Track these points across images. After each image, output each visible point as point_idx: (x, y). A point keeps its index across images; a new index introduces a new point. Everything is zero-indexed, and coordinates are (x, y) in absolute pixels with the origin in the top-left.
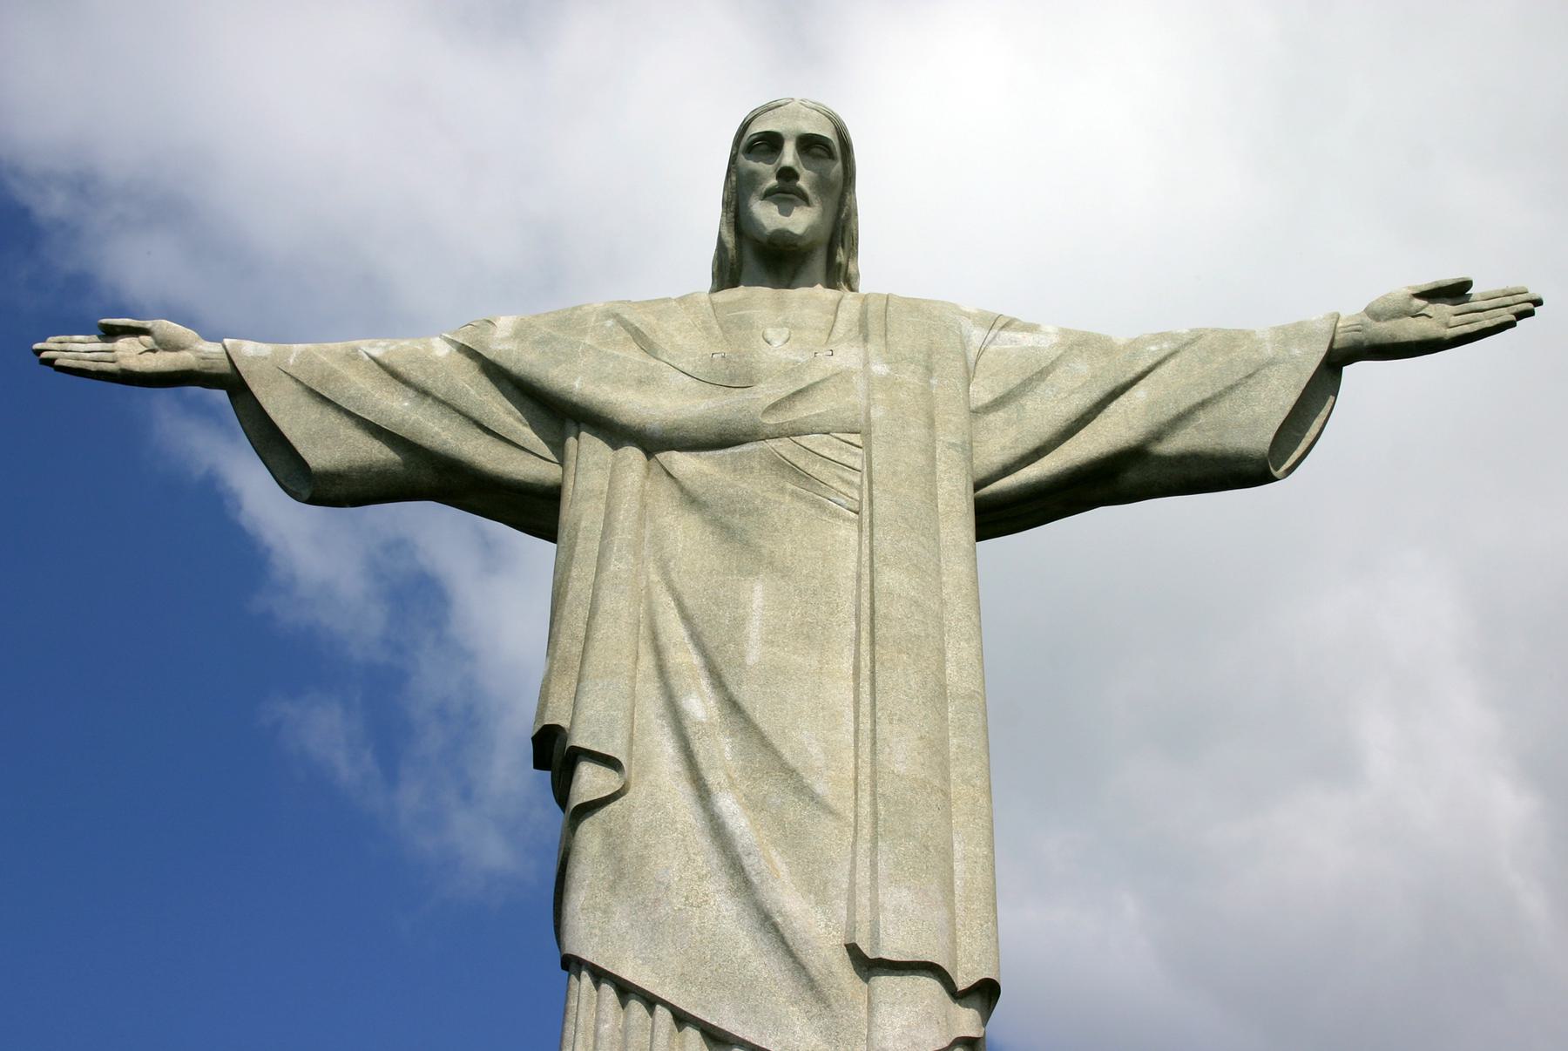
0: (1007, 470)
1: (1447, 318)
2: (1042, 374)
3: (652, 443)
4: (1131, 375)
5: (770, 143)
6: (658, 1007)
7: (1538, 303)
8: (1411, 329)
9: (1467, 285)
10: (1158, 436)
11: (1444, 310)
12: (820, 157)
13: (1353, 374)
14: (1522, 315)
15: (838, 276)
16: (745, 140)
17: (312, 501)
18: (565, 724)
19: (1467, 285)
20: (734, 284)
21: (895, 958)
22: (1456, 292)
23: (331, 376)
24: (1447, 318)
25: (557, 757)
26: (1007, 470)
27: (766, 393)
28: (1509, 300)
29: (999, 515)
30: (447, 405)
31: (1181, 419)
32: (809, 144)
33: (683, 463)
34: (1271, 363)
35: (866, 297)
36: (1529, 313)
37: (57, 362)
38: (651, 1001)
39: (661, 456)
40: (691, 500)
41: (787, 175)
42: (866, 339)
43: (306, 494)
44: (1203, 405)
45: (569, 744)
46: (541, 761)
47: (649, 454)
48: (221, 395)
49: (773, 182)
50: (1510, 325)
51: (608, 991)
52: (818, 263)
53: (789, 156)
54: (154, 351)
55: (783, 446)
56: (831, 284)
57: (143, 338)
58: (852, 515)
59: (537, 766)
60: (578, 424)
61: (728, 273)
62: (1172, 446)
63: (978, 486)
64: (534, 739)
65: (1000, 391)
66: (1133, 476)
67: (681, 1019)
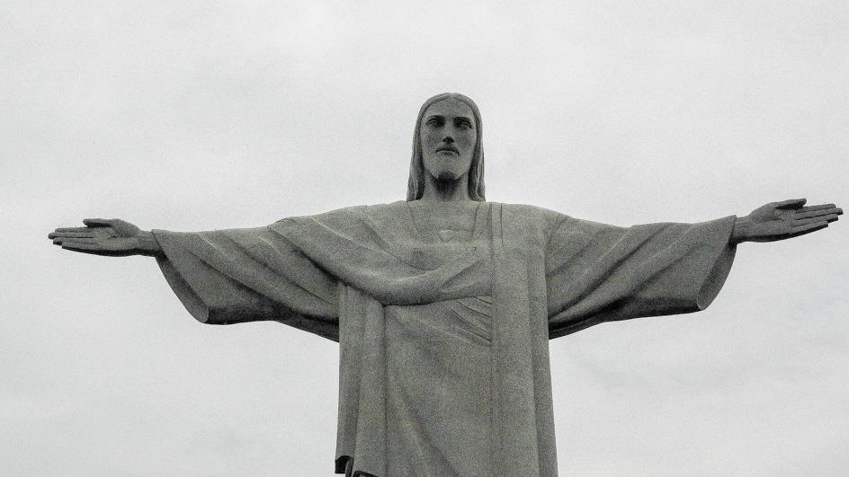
0: (564, 309)
1: (791, 220)
2: (581, 254)
3: (387, 301)
4: (627, 252)
5: (438, 122)
7: (842, 213)
8: (774, 227)
9: (804, 202)
10: (642, 287)
11: (792, 214)
12: (465, 128)
13: (743, 249)
14: (830, 221)
15: (475, 190)
16: (425, 120)
17: (209, 322)
18: (351, 456)
19: (804, 202)
20: (419, 197)
22: (797, 206)
23: (211, 251)
24: (791, 220)
27: (444, 274)
28: (824, 212)
29: (559, 328)
30: (275, 272)
31: (653, 279)
32: (461, 123)
33: (403, 314)
34: (702, 245)
35: (491, 205)
36: (837, 219)
37: (65, 244)
39: (392, 307)
40: (408, 335)
41: (449, 140)
42: (491, 238)
44: (663, 271)
45: (355, 469)
47: (384, 306)
48: (152, 260)
49: (442, 144)
50: (826, 226)
52: (464, 184)
53: (448, 130)
55: (451, 306)
56: (472, 195)
57: (111, 230)
58: (488, 343)
59: (336, 472)
61: (417, 192)
62: (649, 294)
63: (549, 318)
64: (336, 461)
65: (559, 263)
66: (627, 309)
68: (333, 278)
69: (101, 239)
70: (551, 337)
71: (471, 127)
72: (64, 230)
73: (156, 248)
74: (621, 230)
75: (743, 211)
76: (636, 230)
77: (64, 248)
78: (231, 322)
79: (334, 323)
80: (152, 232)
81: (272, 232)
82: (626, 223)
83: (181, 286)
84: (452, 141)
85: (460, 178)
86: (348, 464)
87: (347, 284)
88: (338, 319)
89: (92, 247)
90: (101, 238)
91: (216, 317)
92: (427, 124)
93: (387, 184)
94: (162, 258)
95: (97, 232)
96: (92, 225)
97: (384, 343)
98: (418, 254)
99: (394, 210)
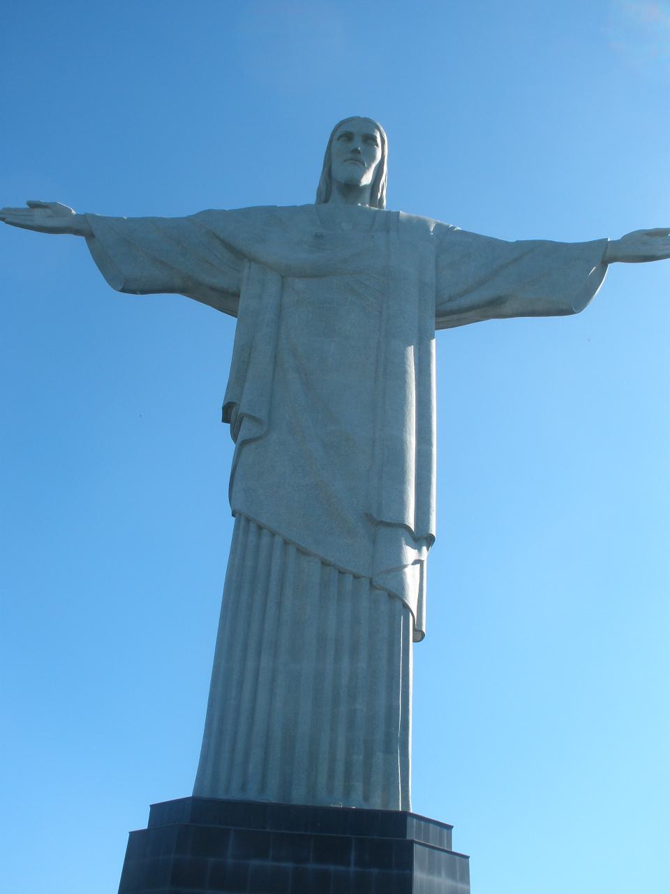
0: (451, 299)
3: (285, 274)
5: (349, 137)
6: (277, 536)
16: (338, 134)
20: (326, 201)
21: (389, 521)
25: (233, 417)
26: (451, 299)
33: (299, 284)
35: (389, 213)
38: (273, 534)
41: (356, 151)
42: (388, 231)
43: (121, 287)
46: (226, 419)
47: (283, 277)
51: (253, 527)
52: (367, 195)
54: (52, 216)
57: (47, 210)
60: (250, 262)
61: (325, 195)
67: (286, 543)
68: (239, 255)
69: (39, 217)
70: (437, 329)
71: (377, 145)
72: (9, 209)
73: (84, 228)
74: (507, 243)
75: (614, 235)
76: (518, 242)
77: (7, 223)
78: (144, 292)
79: (236, 295)
80: (84, 216)
81: (189, 219)
82: (511, 237)
83: (103, 262)
84: (359, 152)
85: (365, 186)
86: (234, 409)
87: (252, 259)
88: (240, 291)
89: (29, 223)
90: (40, 219)
91: (129, 288)
92: (339, 139)
93: (300, 187)
94: (90, 236)
95: (37, 212)
96: (34, 205)
97: (280, 309)
98: (318, 237)
99: (304, 209)
